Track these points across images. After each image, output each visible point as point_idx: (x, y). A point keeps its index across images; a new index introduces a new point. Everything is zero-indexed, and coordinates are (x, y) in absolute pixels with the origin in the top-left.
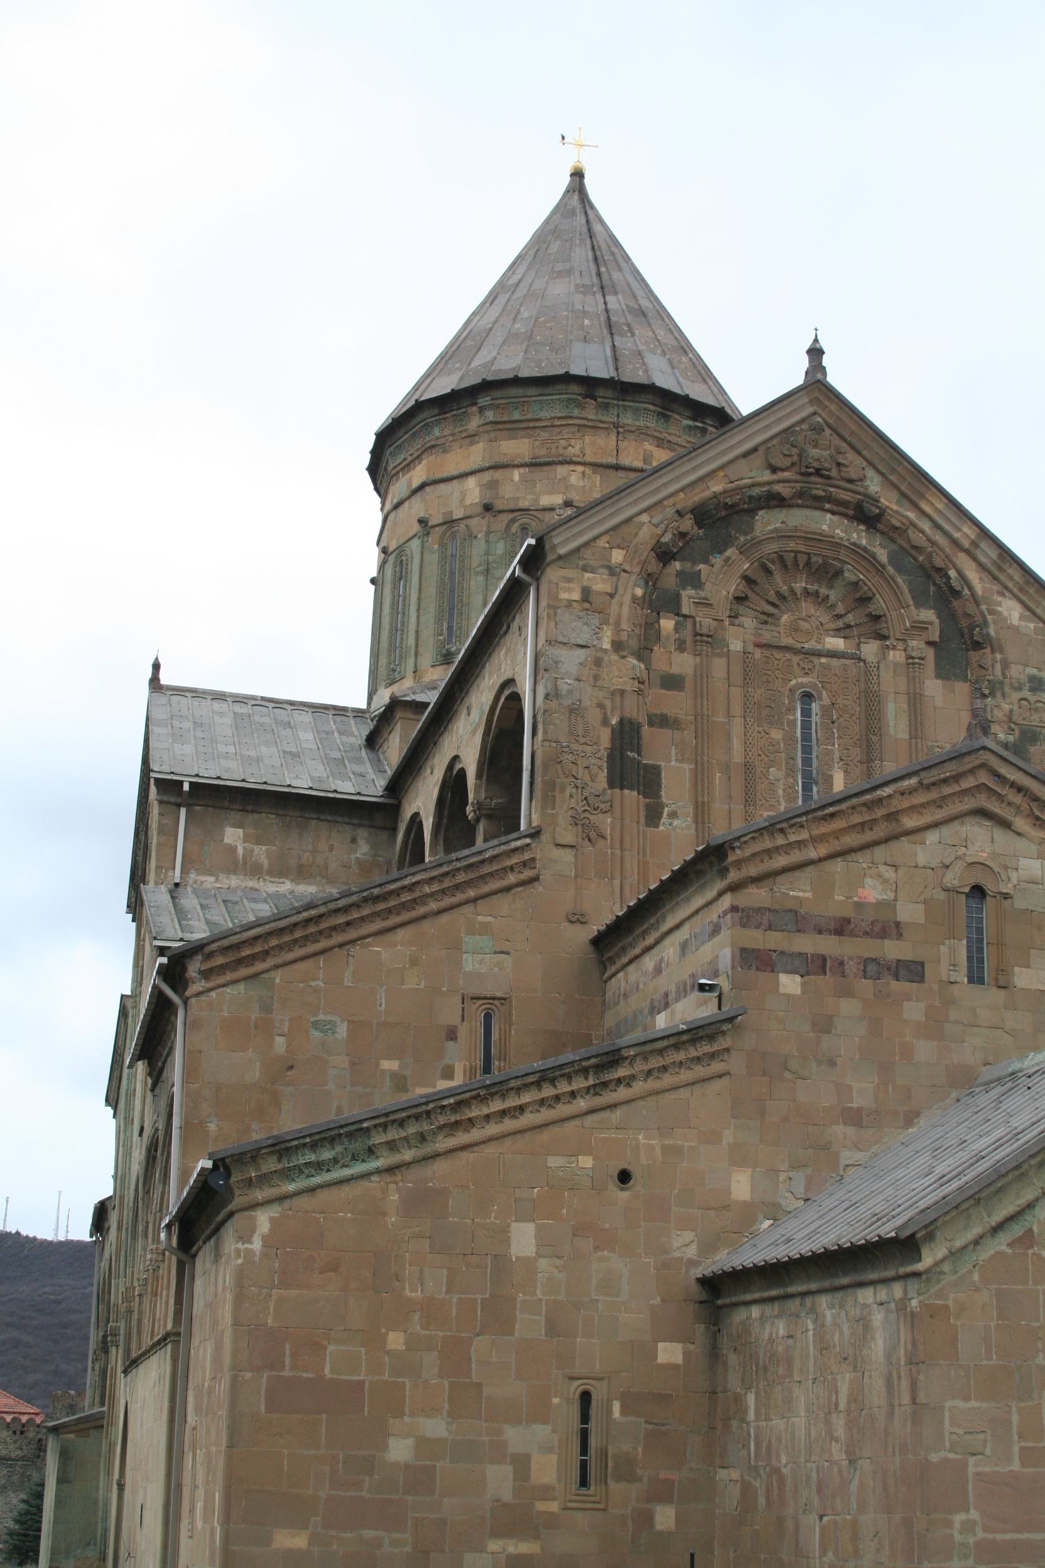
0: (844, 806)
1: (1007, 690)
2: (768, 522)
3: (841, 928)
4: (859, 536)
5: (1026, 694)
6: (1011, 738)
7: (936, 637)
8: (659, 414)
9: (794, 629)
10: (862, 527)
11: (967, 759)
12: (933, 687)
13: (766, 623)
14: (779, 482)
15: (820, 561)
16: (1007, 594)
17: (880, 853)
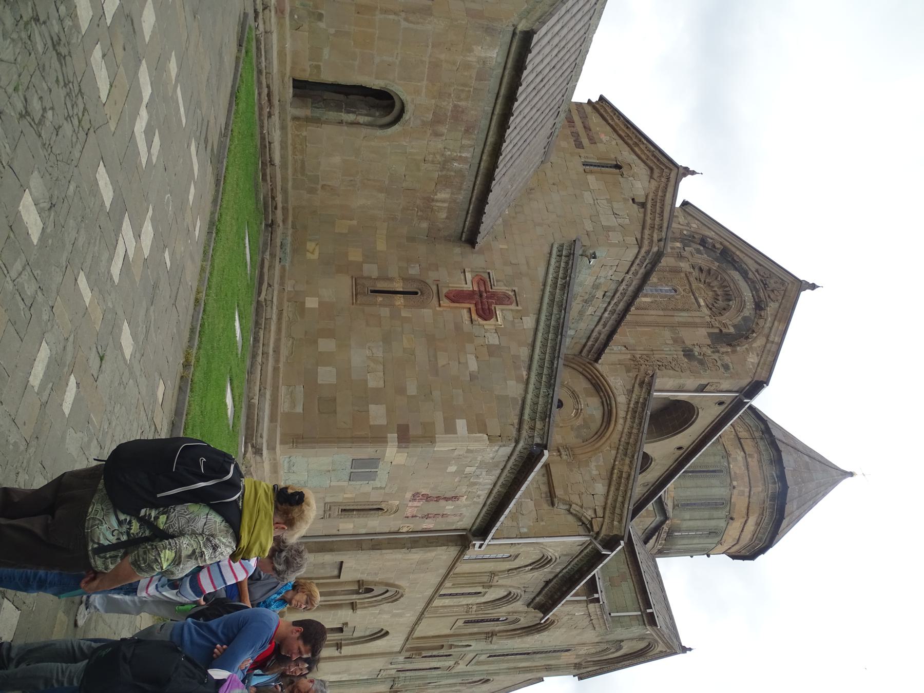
0: (632, 129)
1: (717, 354)
2: (736, 275)
3: (587, 128)
4: (750, 305)
5: (719, 363)
6: (696, 354)
7: (724, 330)
8: (771, 459)
9: (699, 288)
10: (754, 306)
11: (671, 165)
12: (703, 332)
13: (696, 279)
14: (753, 273)
15: (731, 293)
16: (759, 357)
17: (620, 142)
